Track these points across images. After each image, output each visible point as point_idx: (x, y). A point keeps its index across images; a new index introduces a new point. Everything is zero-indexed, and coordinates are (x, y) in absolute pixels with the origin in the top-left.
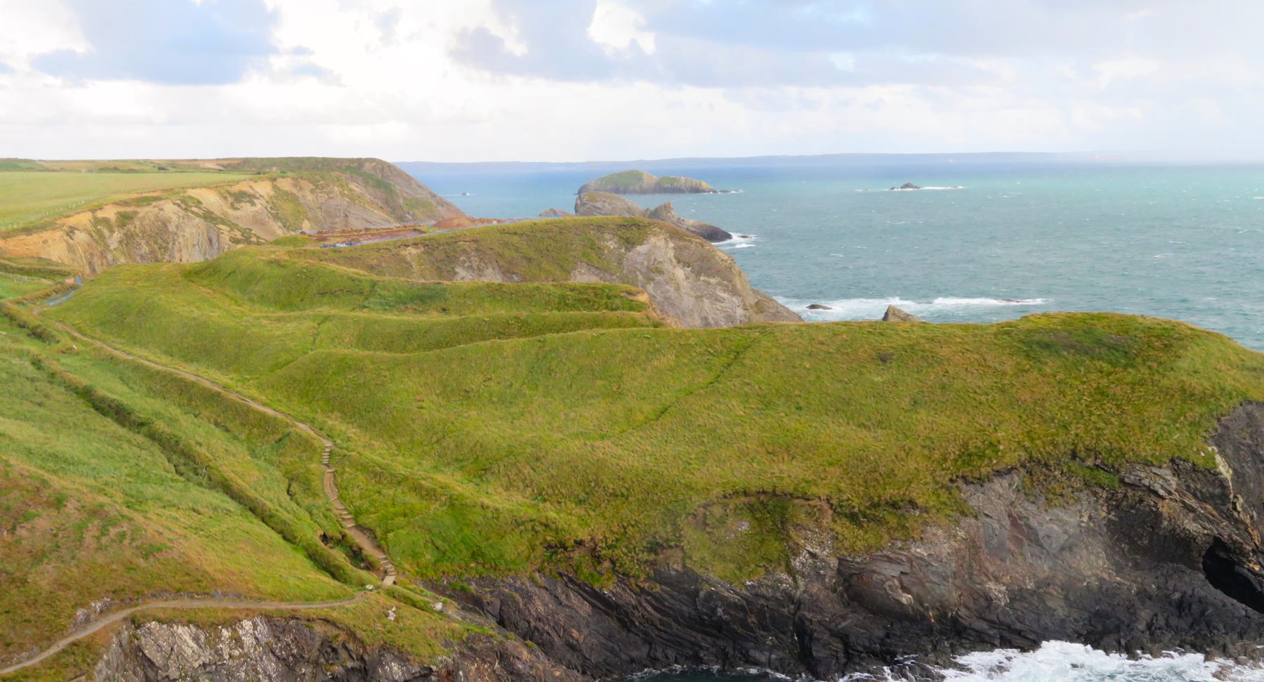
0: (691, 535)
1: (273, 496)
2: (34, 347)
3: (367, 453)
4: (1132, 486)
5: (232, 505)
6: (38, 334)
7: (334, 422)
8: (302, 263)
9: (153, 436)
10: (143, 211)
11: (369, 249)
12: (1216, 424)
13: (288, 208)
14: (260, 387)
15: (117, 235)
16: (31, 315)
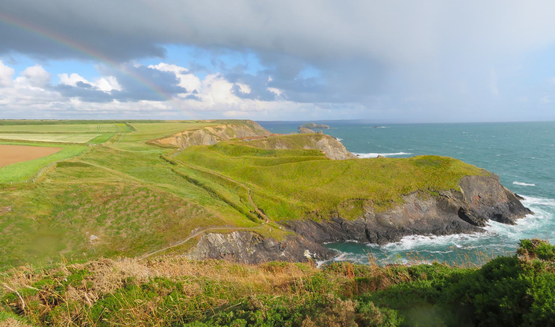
1: (237, 202)
2: (172, 166)
3: (259, 191)
5: (226, 204)
6: (172, 163)
7: (250, 183)
8: (238, 145)
9: (205, 188)
10: (195, 132)
11: (254, 141)
13: (230, 132)
14: (231, 175)
15: (188, 138)
16: (170, 158)
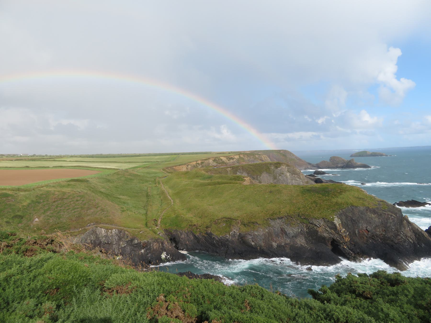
0: (213, 225)
4: (311, 223)
7: (178, 201)
12: (341, 211)
